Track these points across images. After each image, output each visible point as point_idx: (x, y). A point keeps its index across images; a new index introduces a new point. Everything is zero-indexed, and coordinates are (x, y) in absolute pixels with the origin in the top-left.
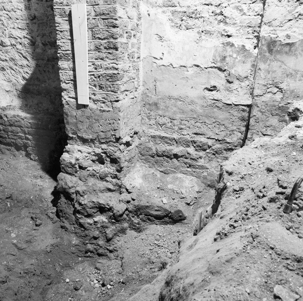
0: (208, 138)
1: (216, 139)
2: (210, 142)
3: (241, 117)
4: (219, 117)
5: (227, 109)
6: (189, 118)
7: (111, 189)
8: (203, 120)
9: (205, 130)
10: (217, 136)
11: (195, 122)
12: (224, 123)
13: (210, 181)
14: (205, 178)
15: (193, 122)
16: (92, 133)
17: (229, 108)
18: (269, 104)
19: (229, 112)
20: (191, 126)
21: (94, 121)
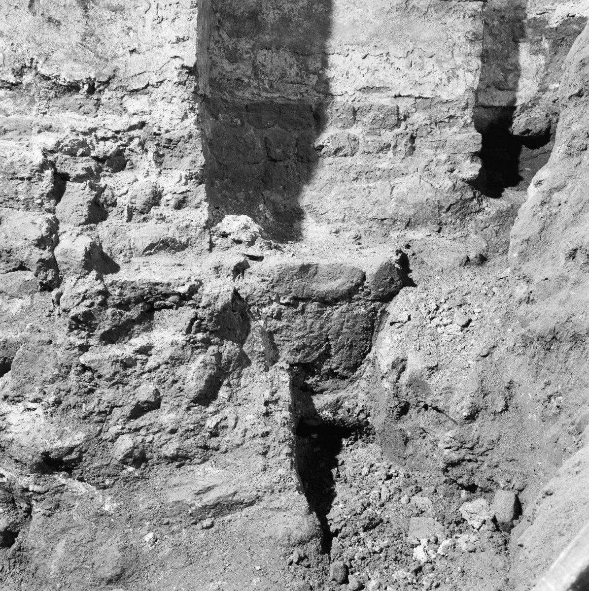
0: (396, 97)
1: (417, 96)
2: (404, 105)
3: (471, 33)
4: (422, 38)
5: (440, 14)
6: (347, 47)
7: (173, 241)
8: (383, 48)
9: (388, 74)
10: (419, 88)
11: (364, 54)
12: (433, 50)
13: (415, 206)
14: (402, 201)
15: (357, 56)
16: (97, 60)
17: (443, 12)
18: (507, 16)
19: (444, 20)
20: (354, 70)
21: (107, 14)
